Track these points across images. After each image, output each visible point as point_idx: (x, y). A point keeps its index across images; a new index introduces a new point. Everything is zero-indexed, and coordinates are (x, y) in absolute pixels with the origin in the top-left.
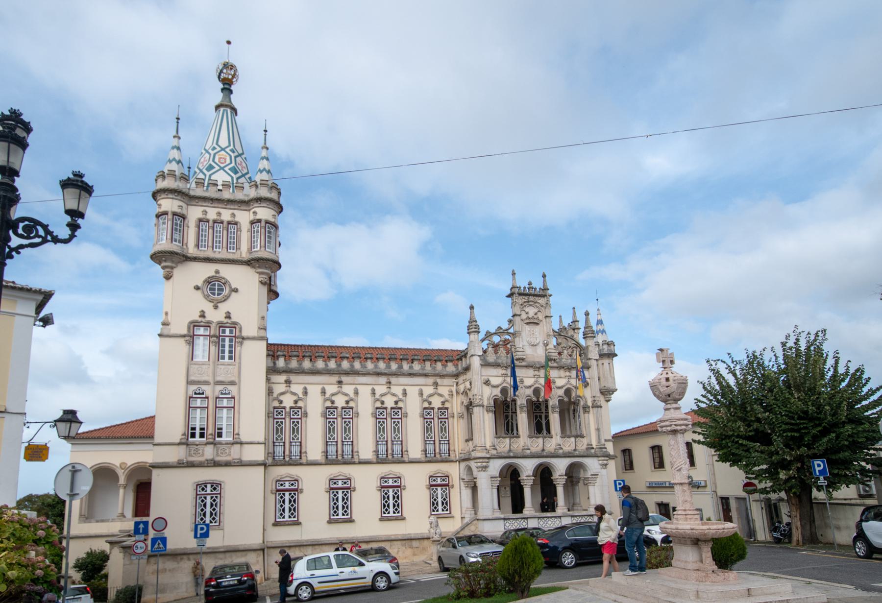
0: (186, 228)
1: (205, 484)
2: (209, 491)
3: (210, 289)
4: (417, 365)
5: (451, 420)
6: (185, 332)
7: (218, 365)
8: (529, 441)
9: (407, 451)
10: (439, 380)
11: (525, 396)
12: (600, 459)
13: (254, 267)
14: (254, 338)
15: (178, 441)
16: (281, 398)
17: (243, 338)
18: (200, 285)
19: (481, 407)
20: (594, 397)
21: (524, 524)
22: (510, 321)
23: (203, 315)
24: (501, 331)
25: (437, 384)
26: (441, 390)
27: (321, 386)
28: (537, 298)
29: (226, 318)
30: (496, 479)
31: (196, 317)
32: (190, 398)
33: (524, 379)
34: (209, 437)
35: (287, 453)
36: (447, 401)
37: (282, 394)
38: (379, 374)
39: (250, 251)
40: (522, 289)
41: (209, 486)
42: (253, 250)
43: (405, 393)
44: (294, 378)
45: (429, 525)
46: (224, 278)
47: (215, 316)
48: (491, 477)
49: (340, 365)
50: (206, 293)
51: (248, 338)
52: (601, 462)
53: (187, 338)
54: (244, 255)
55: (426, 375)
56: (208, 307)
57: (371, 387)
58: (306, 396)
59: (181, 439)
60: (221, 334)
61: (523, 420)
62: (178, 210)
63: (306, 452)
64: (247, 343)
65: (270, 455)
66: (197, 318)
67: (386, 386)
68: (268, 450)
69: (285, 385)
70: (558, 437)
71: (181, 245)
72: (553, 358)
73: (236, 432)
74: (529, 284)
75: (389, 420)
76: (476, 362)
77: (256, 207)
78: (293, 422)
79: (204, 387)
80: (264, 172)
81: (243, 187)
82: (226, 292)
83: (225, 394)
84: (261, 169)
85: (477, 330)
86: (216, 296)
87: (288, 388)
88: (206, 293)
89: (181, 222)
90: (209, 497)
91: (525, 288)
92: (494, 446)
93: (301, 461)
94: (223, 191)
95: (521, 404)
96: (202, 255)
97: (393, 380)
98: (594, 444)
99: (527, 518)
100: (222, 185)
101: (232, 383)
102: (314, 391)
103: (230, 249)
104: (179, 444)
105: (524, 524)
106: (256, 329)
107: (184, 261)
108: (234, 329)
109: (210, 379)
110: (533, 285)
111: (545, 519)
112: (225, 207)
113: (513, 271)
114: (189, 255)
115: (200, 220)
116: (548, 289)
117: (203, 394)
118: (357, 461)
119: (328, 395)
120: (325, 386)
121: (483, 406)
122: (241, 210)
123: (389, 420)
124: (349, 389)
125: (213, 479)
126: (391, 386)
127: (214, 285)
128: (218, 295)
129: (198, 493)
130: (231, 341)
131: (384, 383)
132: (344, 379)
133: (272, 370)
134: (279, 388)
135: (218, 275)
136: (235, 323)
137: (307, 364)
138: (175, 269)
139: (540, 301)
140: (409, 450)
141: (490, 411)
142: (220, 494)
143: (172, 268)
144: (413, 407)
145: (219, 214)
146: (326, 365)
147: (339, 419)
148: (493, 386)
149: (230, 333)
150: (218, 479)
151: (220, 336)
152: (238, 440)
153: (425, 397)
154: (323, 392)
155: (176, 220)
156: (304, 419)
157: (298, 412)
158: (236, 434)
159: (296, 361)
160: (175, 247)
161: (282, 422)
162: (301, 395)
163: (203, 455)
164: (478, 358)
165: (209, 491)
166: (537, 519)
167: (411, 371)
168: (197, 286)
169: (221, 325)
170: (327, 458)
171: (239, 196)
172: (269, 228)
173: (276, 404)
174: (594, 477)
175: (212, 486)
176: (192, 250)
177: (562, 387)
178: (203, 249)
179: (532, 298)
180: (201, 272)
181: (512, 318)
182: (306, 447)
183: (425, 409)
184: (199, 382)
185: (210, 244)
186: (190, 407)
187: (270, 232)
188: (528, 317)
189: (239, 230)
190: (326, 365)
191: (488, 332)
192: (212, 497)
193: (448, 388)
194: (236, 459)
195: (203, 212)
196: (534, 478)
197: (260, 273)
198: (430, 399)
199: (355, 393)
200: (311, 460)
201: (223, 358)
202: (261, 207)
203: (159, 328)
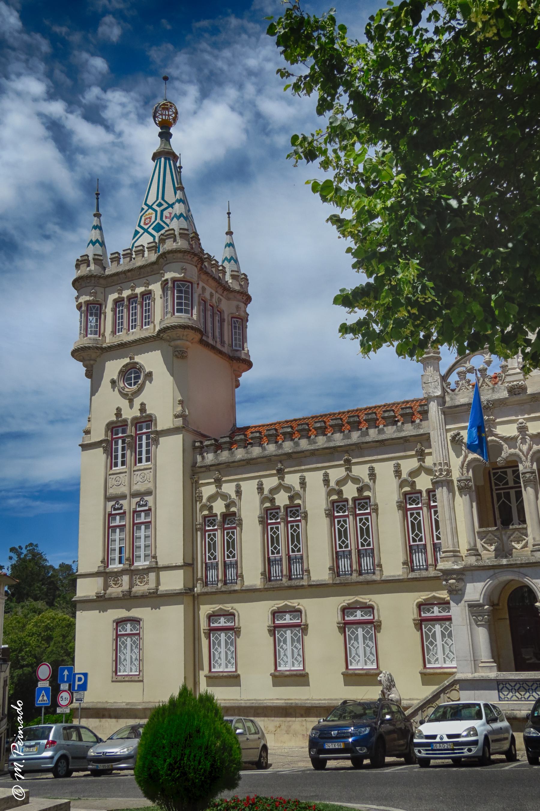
0: (103, 316)
6: (103, 437)
7: (134, 471)
9: (380, 565)
15: (95, 570)
18: (115, 378)
26: (429, 461)
32: (110, 515)
56: (124, 404)
59: (99, 567)
66: (114, 418)
80: (175, 218)
86: (133, 387)
89: (97, 310)
103: (145, 326)
106: (171, 417)
107: (102, 354)
108: (150, 422)
109: (124, 490)
117: (121, 508)
129: (119, 633)
130: (147, 438)
134: (208, 491)
136: (150, 416)
140: (382, 562)
143: (92, 366)
152: (154, 565)
155: (91, 310)
169: (137, 423)
176: (109, 340)
182: (242, 568)
183: (405, 494)
185: (125, 326)
200: (247, 586)
201: (140, 461)
202: (168, 264)
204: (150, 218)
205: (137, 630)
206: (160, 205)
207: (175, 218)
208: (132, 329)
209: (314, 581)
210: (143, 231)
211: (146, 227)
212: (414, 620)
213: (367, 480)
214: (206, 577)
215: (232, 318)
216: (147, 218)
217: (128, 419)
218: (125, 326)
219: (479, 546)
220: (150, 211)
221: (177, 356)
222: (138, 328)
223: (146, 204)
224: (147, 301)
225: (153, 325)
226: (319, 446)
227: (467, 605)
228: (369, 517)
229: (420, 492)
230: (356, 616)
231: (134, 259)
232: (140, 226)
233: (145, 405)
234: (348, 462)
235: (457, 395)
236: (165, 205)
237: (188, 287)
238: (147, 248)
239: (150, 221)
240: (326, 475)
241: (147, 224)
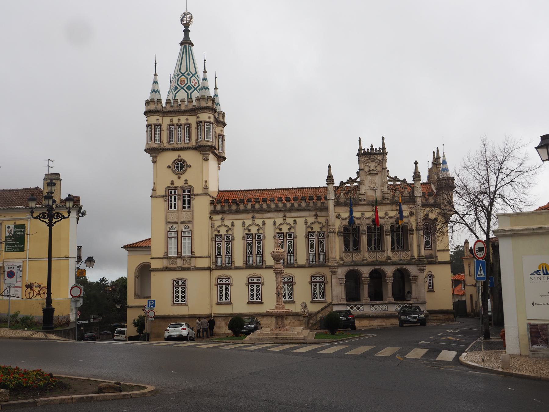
0: (162, 131)
1: (178, 280)
2: (180, 284)
3: (177, 167)
4: (304, 204)
5: (326, 239)
6: (163, 193)
7: (182, 212)
8: (367, 255)
9: (296, 260)
10: (318, 213)
11: (365, 225)
12: (419, 266)
13: (199, 151)
14: (201, 195)
15: (162, 256)
16: (219, 229)
17: (195, 195)
18: (170, 165)
21: (361, 308)
22: (358, 173)
23: (172, 183)
24: (351, 181)
25: (317, 215)
27: (242, 221)
28: (376, 156)
29: (185, 183)
31: (169, 184)
34: (179, 254)
35: (224, 262)
36: (324, 227)
37: (219, 226)
38: (277, 210)
39: (197, 142)
40: (366, 150)
41: (180, 281)
42: (198, 140)
43: (295, 222)
44: (226, 217)
45: (301, 307)
46: (183, 160)
47: (179, 183)
48: (339, 278)
49: (254, 206)
50: (174, 170)
51: (198, 195)
52: (419, 268)
53: (165, 198)
54: (194, 144)
55: (310, 210)
57: (273, 220)
58: (234, 227)
59: (164, 255)
60: (183, 194)
61: (364, 239)
62: (155, 122)
63: (234, 262)
64: (197, 198)
65: (213, 263)
66: (169, 185)
67: (283, 219)
68: (213, 260)
69: (221, 221)
70: (389, 251)
71: (160, 142)
72: (386, 197)
73: (193, 251)
74: (371, 146)
75: (285, 240)
76: (331, 204)
77: (199, 113)
78: (227, 243)
79: (175, 225)
80: (204, 89)
81: (193, 101)
82: (184, 169)
83: (186, 229)
84: (202, 87)
85: (332, 182)
87: (223, 223)
88: (174, 170)
89: (159, 129)
90: (180, 288)
91: (368, 149)
92: (342, 258)
93: (231, 267)
94: (181, 106)
95: (362, 231)
96: (171, 146)
97: (288, 214)
98: (416, 255)
99: (363, 305)
100: (181, 102)
101: (190, 222)
102: (238, 224)
104: (163, 258)
105: (361, 308)
107: (162, 151)
110: (374, 147)
112: (182, 115)
113: (360, 138)
114: (164, 148)
115: (170, 125)
116: (386, 149)
118: (264, 266)
119: (246, 226)
120: (245, 220)
121: (335, 233)
122: (192, 115)
123: (285, 240)
124: (259, 222)
125: (182, 277)
126: (286, 219)
127: (178, 164)
128: (180, 170)
129: (175, 285)
131: (282, 216)
132: (257, 215)
133: (214, 212)
134: (217, 223)
135: (180, 158)
136: (190, 186)
137: (234, 207)
138: (157, 157)
139: (379, 158)
140: (297, 259)
141: (340, 235)
142: (186, 286)
143: (156, 157)
144: (301, 231)
145: (179, 120)
146: (245, 207)
147: (254, 241)
148: (343, 219)
149: (188, 193)
150: (184, 277)
151: (182, 195)
152: (194, 255)
153: (309, 224)
154: (244, 224)
156: (233, 241)
157: (230, 237)
158: (192, 252)
159: (227, 206)
160: (155, 146)
161: (220, 244)
162: (230, 227)
163: (176, 264)
164: (332, 201)
165: (180, 284)
167: (300, 208)
168: (169, 166)
169: (183, 188)
170: (247, 265)
171: (190, 107)
172: (207, 125)
173: (216, 233)
174: (414, 278)
175: (181, 281)
176: (165, 144)
178: (172, 143)
179: (372, 157)
180: (171, 157)
181: (359, 171)
183: (309, 232)
184: (172, 222)
185: (176, 140)
186: (168, 237)
187: (207, 128)
188: (369, 170)
189: (191, 128)
190: (245, 207)
191: (342, 182)
192: (181, 288)
193: (325, 218)
194: (193, 266)
195: (170, 120)
196: (369, 279)
197: (203, 154)
198: (312, 226)
199: (263, 224)
200: (237, 267)
201: (185, 207)
203: (150, 193)
204: (184, 81)
205: (184, 284)
206: (188, 74)
207: (204, 89)
208: (179, 141)
209: (267, 266)
210: (180, 88)
211: (182, 86)
212: (309, 282)
213: (292, 225)
214: (216, 262)
215: (219, 135)
216: (182, 81)
217: (178, 187)
218: (176, 140)
219: (344, 257)
220: (183, 77)
221: (204, 160)
222: (184, 142)
223: (180, 72)
224: (187, 129)
225: (191, 142)
226: (272, 209)
228: (293, 240)
229: (314, 232)
230: (285, 280)
231: (180, 105)
232: (177, 84)
233: (187, 181)
234: (285, 216)
235: (340, 199)
236: (191, 75)
237: (210, 126)
238: (188, 101)
239: (184, 83)
240: (275, 221)
241: (182, 84)
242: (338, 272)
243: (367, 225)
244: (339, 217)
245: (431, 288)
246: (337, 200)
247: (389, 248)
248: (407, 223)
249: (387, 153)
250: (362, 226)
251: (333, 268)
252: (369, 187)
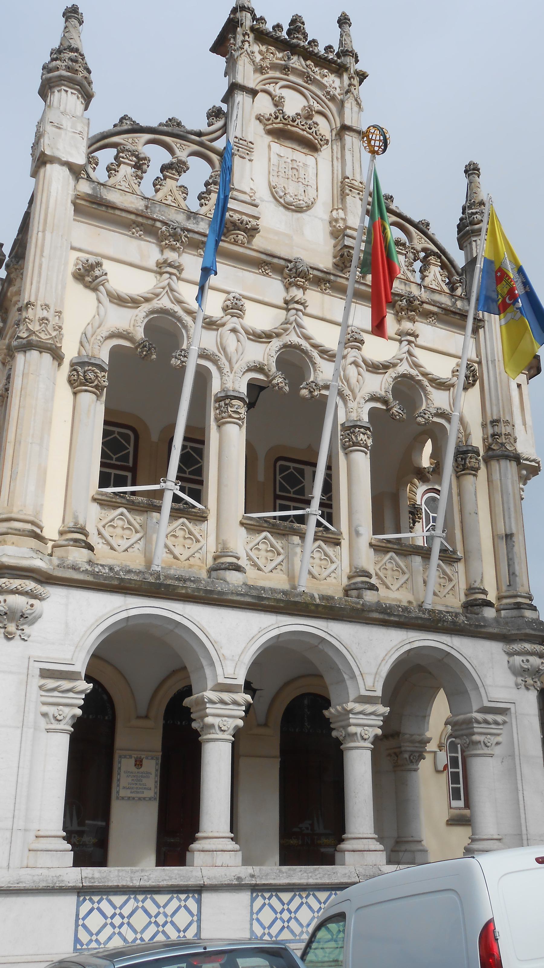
12: (517, 647)
19: (47, 357)
20: (495, 422)
21: (182, 919)
30: (66, 685)
33: (248, 305)
48: (46, 674)
52: (518, 660)
92: (83, 531)
111: (286, 896)
121: (58, 357)
164: (65, 171)
166: (245, 897)
174: (490, 717)
177: (385, 367)
179: (296, 62)
196: (248, 698)
219: (91, 529)
227: (38, 672)
242: (36, 626)
243: (249, 370)
244: (97, 272)
245: (461, 803)
246: (94, 189)
247: (362, 530)
248: (442, 415)
249: (362, 76)
250: (227, 369)
251: (16, 583)
252: (272, 189)
